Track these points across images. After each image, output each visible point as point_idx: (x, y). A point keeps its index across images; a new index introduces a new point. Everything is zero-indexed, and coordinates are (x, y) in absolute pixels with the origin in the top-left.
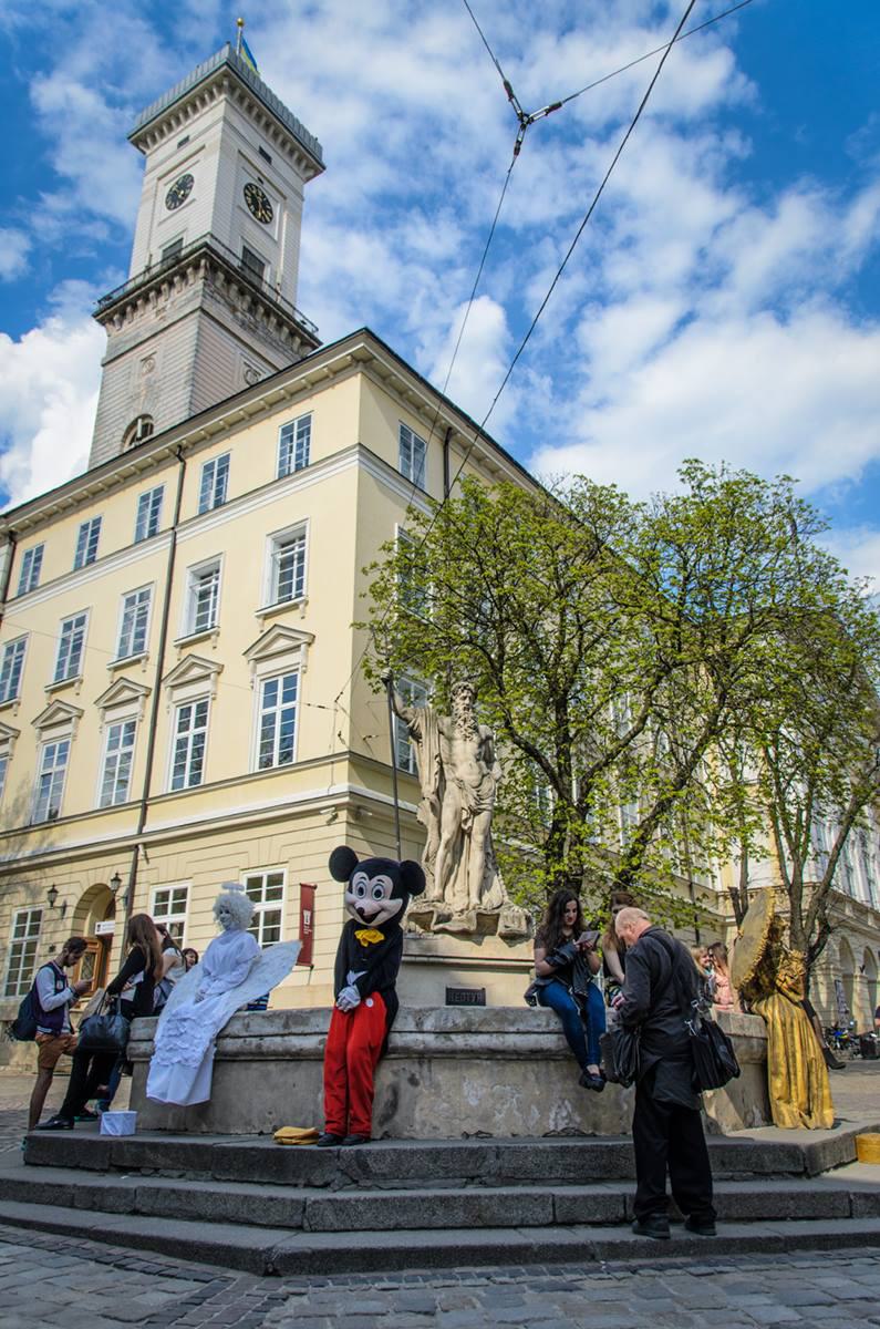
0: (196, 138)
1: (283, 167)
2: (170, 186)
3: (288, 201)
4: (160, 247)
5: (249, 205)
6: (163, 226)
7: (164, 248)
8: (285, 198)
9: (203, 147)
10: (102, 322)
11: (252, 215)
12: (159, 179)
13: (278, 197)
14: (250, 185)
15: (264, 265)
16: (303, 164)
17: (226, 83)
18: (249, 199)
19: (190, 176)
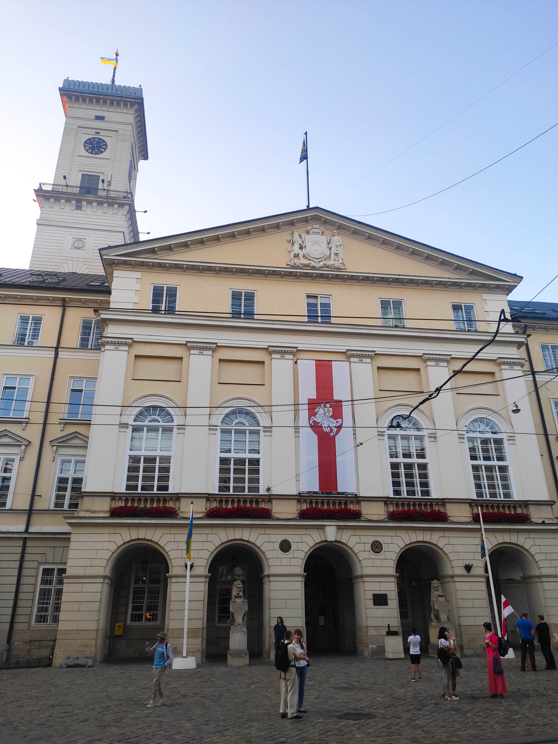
6: (79, 158)
8: (135, 169)
9: (117, 131)
12: (78, 127)
16: (142, 154)
17: (136, 107)
19: (104, 141)
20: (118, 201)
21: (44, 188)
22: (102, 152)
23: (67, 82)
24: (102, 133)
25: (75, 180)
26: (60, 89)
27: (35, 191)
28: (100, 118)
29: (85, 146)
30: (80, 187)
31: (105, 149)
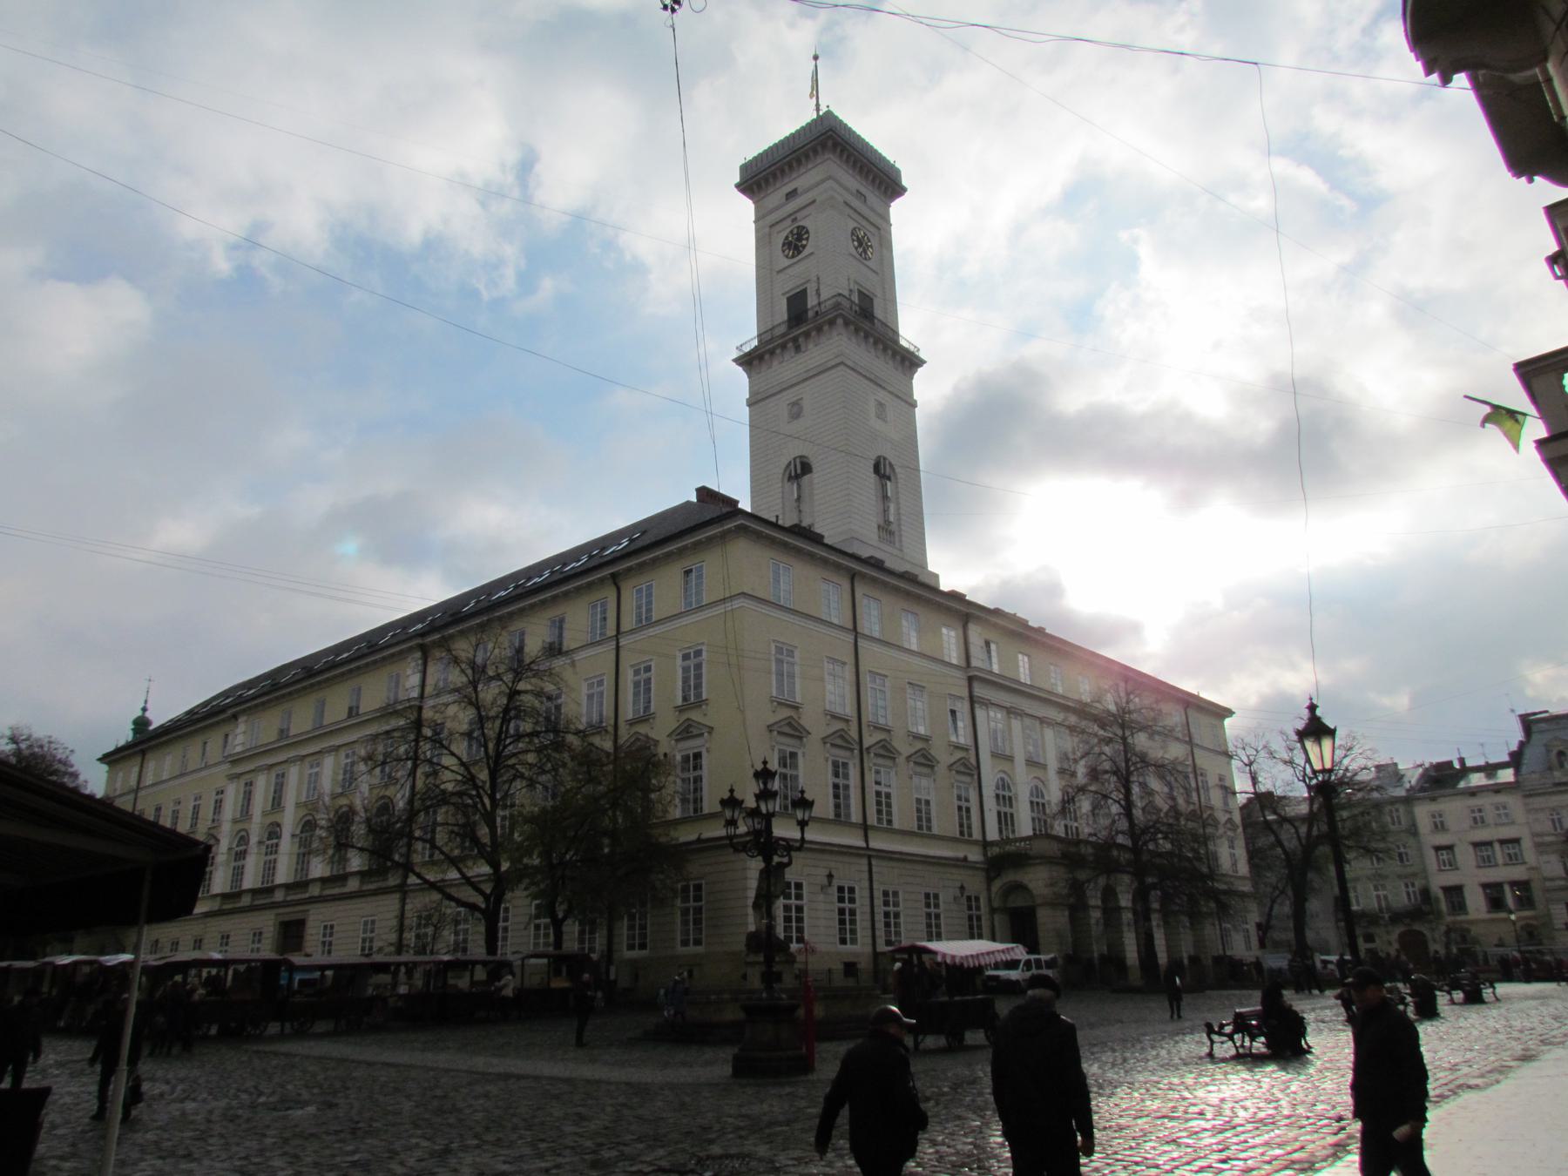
0: (802, 194)
1: (873, 198)
2: (784, 234)
3: (882, 232)
4: (783, 294)
5: (856, 248)
7: (788, 295)
8: (879, 229)
9: (814, 202)
10: (740, 365)
11: (858, 256)
13: (872, 229)
14: (855, 229)
15: (872, 300)
17: (830, 143)
18: (856, 243)
19: (804, 227)
20: (826, 318)
21: (747, 349)
22: (804, 247)
23: (745, 168)
24: (799, 215)
25: (782, 313)
26: (738, 186)
27: (735, 360)
28: (792, 194)
29: (784, 251)
30: (790, 319)
31: (807, 239)
